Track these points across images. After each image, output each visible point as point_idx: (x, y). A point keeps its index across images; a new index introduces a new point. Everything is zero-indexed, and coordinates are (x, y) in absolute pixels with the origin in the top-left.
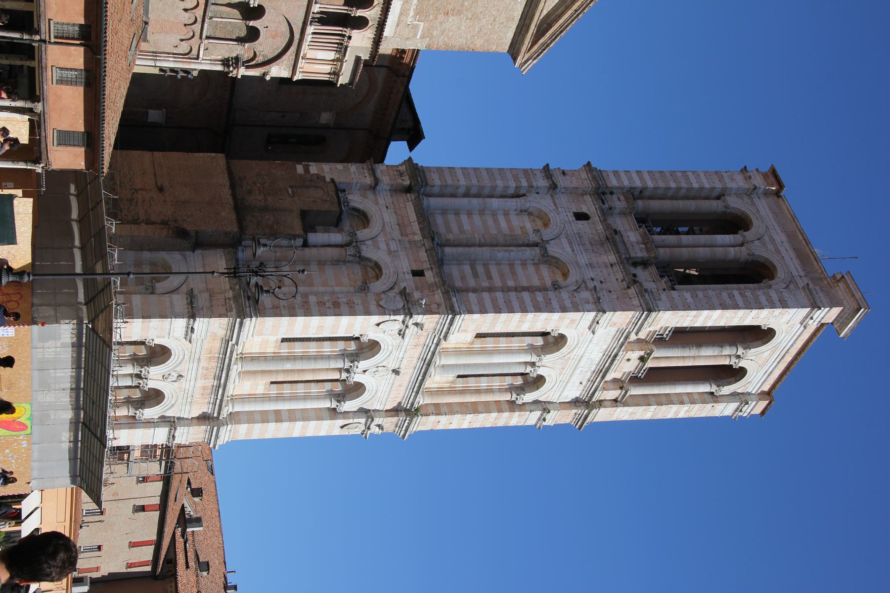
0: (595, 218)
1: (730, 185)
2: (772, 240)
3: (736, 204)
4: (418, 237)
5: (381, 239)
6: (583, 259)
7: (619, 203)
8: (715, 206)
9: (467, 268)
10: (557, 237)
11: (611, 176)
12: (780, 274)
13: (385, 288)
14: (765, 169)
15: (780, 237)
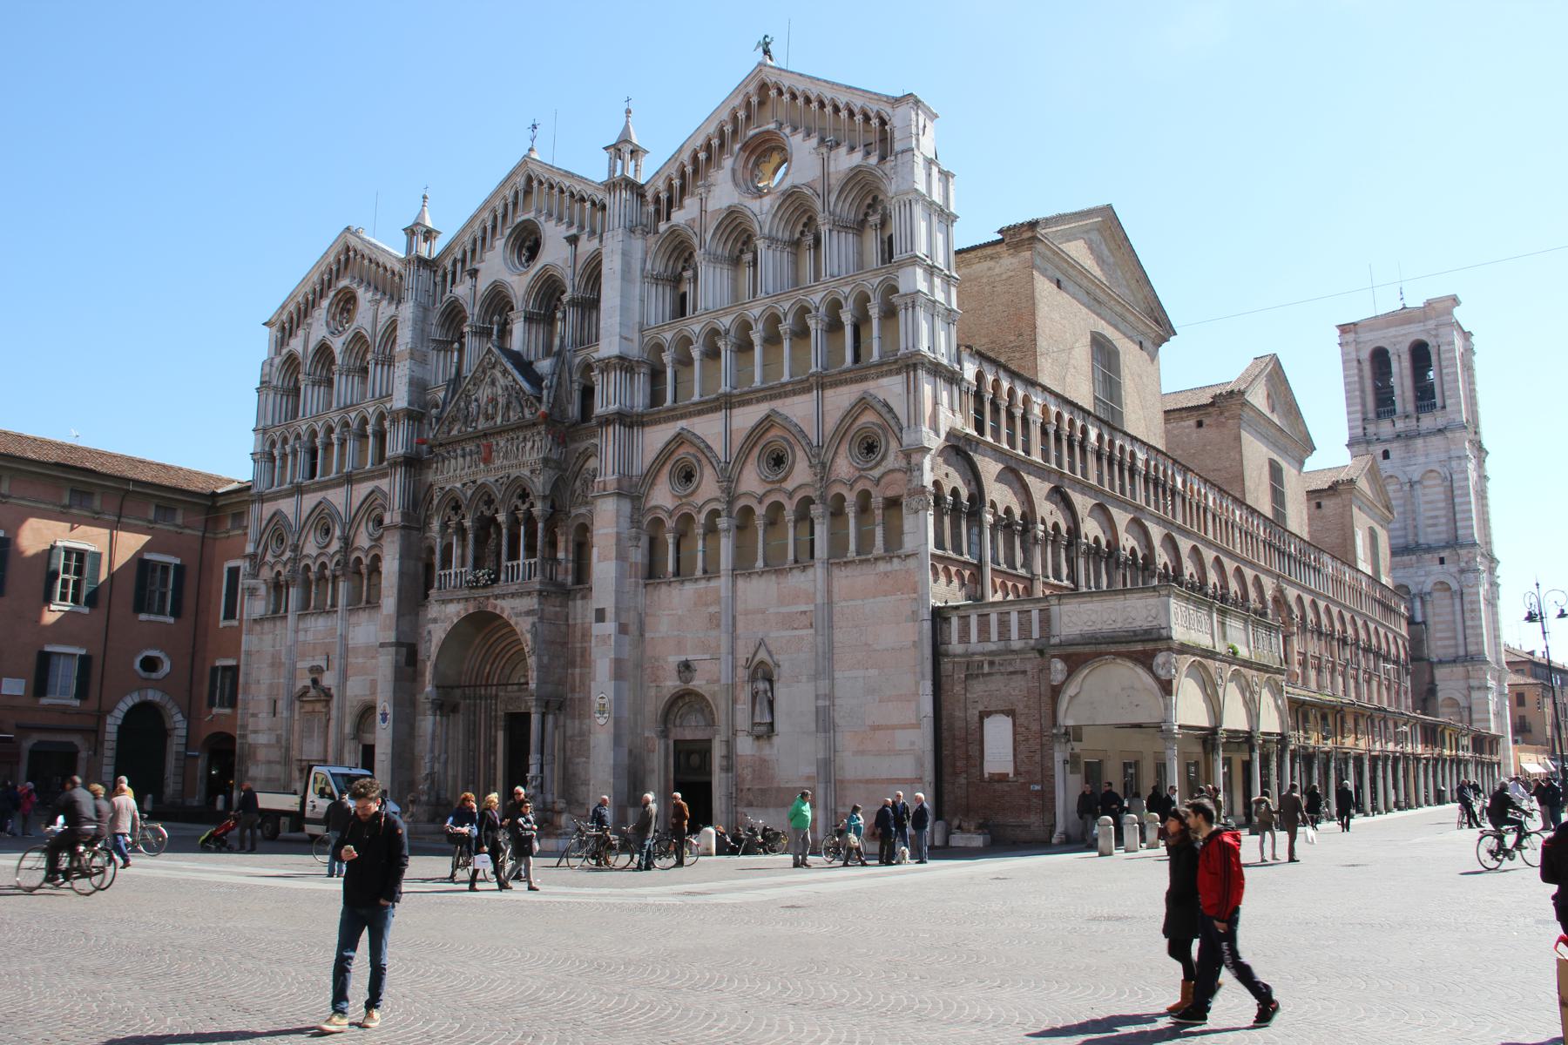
0: (1387, 446)
1: (1353, 355)
2: (1395, 337)
3: (1365, 354)
4: (1414, 557)
5: (1417, 579)
6: (1421, 460)
7: (1371, 429)
8: (1367, 367)
9: (1430, 530)
10: (1405, 473)
11: (1354, 431)
12: (1424, 337)
13: (1455, 581)
14: (1337, 332)
15: (1392, 331)
